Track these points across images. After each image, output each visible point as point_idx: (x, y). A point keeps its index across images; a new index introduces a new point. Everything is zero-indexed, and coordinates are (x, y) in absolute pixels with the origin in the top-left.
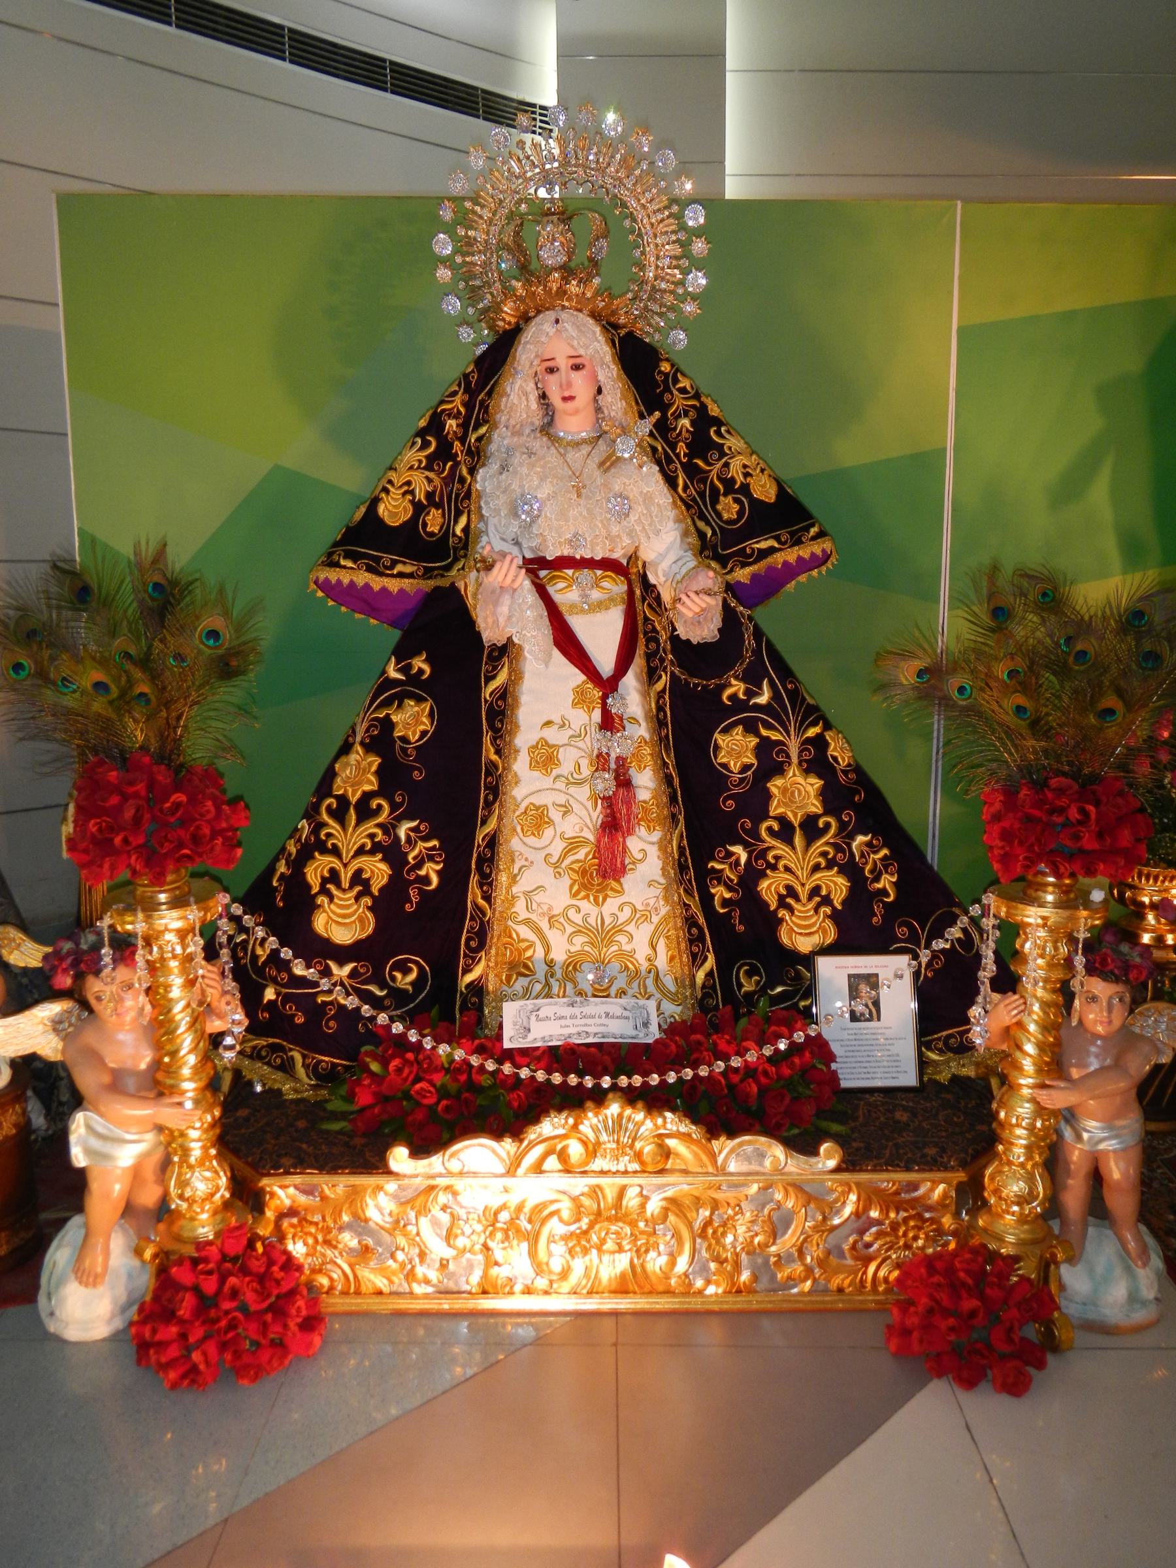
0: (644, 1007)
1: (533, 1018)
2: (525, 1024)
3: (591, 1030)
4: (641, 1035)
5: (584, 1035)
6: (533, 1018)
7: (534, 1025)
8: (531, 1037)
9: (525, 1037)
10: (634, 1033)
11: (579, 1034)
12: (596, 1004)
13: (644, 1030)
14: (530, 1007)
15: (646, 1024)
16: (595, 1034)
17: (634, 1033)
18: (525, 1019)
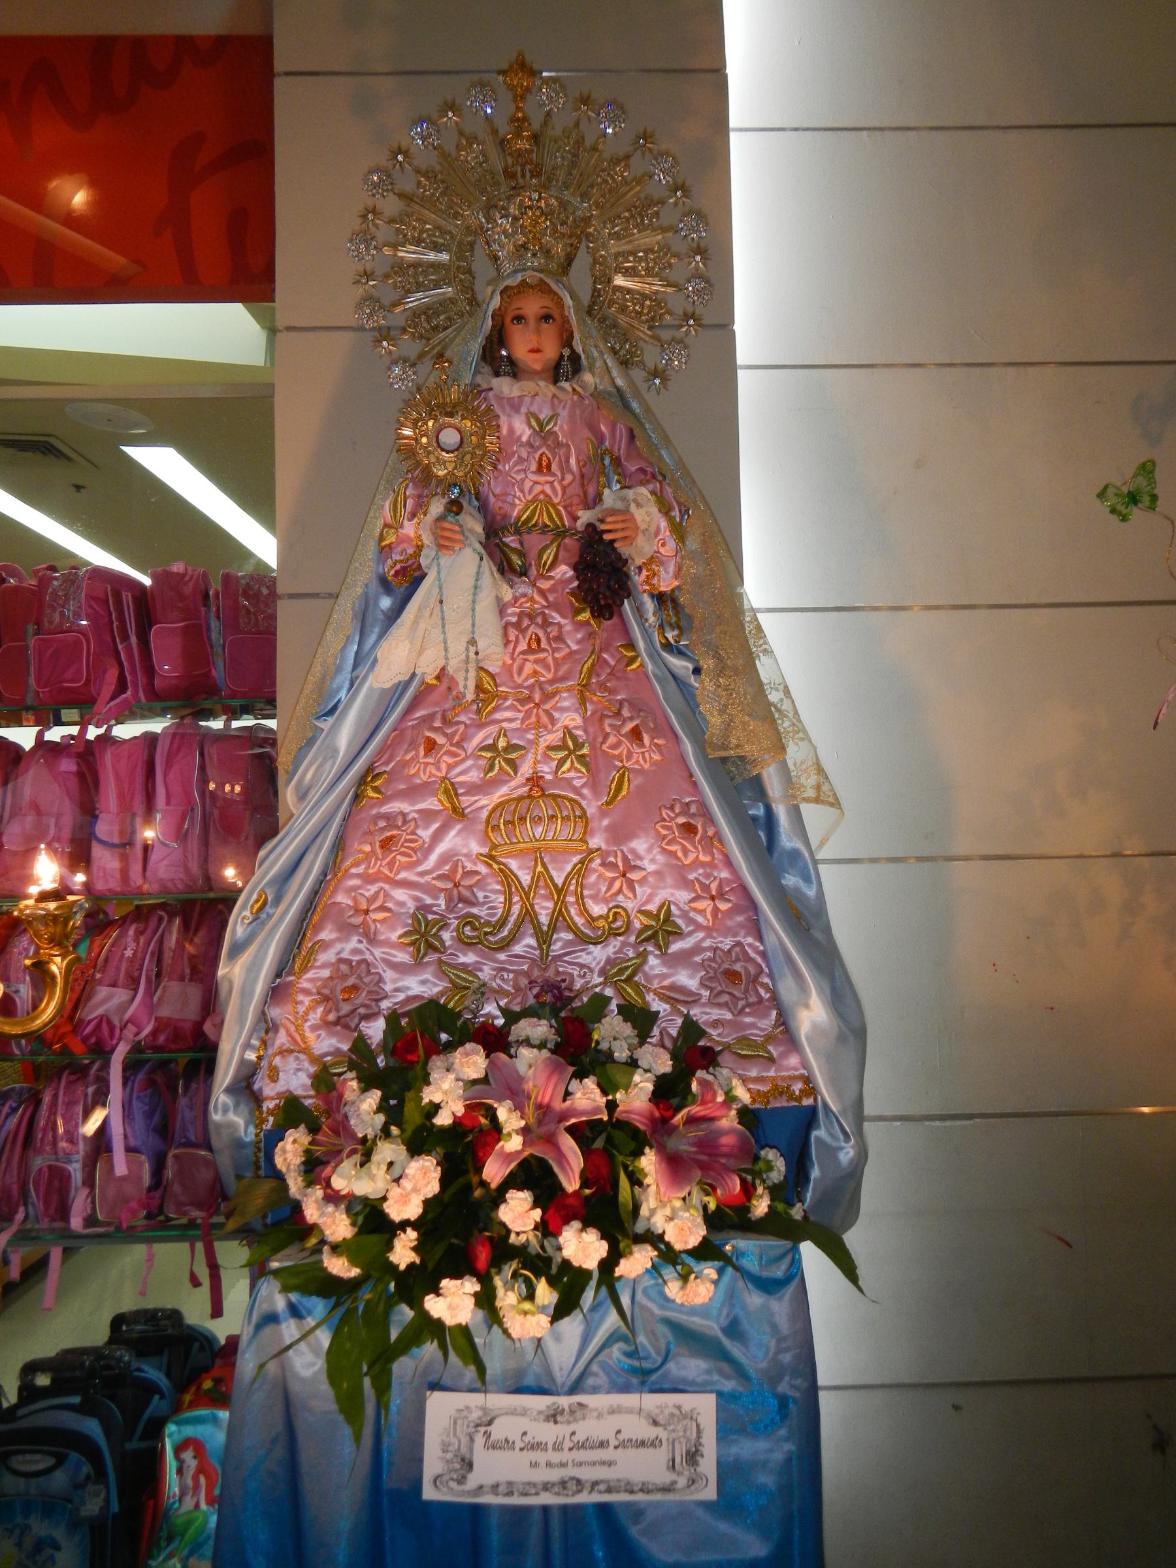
0: (691, 1416)
1: (480, 1440)
2: (464, 1450)
3: (587, 1474)
4: (682, 1482)
5: (572, 1486)
6: (480, 1440)
7: (480, 1455)
8: (473, 1481)
9: (462, 1480)
11: (563, 1483)
12: (600, 1416)
14: (476, 1415)
15: (693, 1457)
16: (595, 1484)
17: (666, 1477)
18: (465, 1440)
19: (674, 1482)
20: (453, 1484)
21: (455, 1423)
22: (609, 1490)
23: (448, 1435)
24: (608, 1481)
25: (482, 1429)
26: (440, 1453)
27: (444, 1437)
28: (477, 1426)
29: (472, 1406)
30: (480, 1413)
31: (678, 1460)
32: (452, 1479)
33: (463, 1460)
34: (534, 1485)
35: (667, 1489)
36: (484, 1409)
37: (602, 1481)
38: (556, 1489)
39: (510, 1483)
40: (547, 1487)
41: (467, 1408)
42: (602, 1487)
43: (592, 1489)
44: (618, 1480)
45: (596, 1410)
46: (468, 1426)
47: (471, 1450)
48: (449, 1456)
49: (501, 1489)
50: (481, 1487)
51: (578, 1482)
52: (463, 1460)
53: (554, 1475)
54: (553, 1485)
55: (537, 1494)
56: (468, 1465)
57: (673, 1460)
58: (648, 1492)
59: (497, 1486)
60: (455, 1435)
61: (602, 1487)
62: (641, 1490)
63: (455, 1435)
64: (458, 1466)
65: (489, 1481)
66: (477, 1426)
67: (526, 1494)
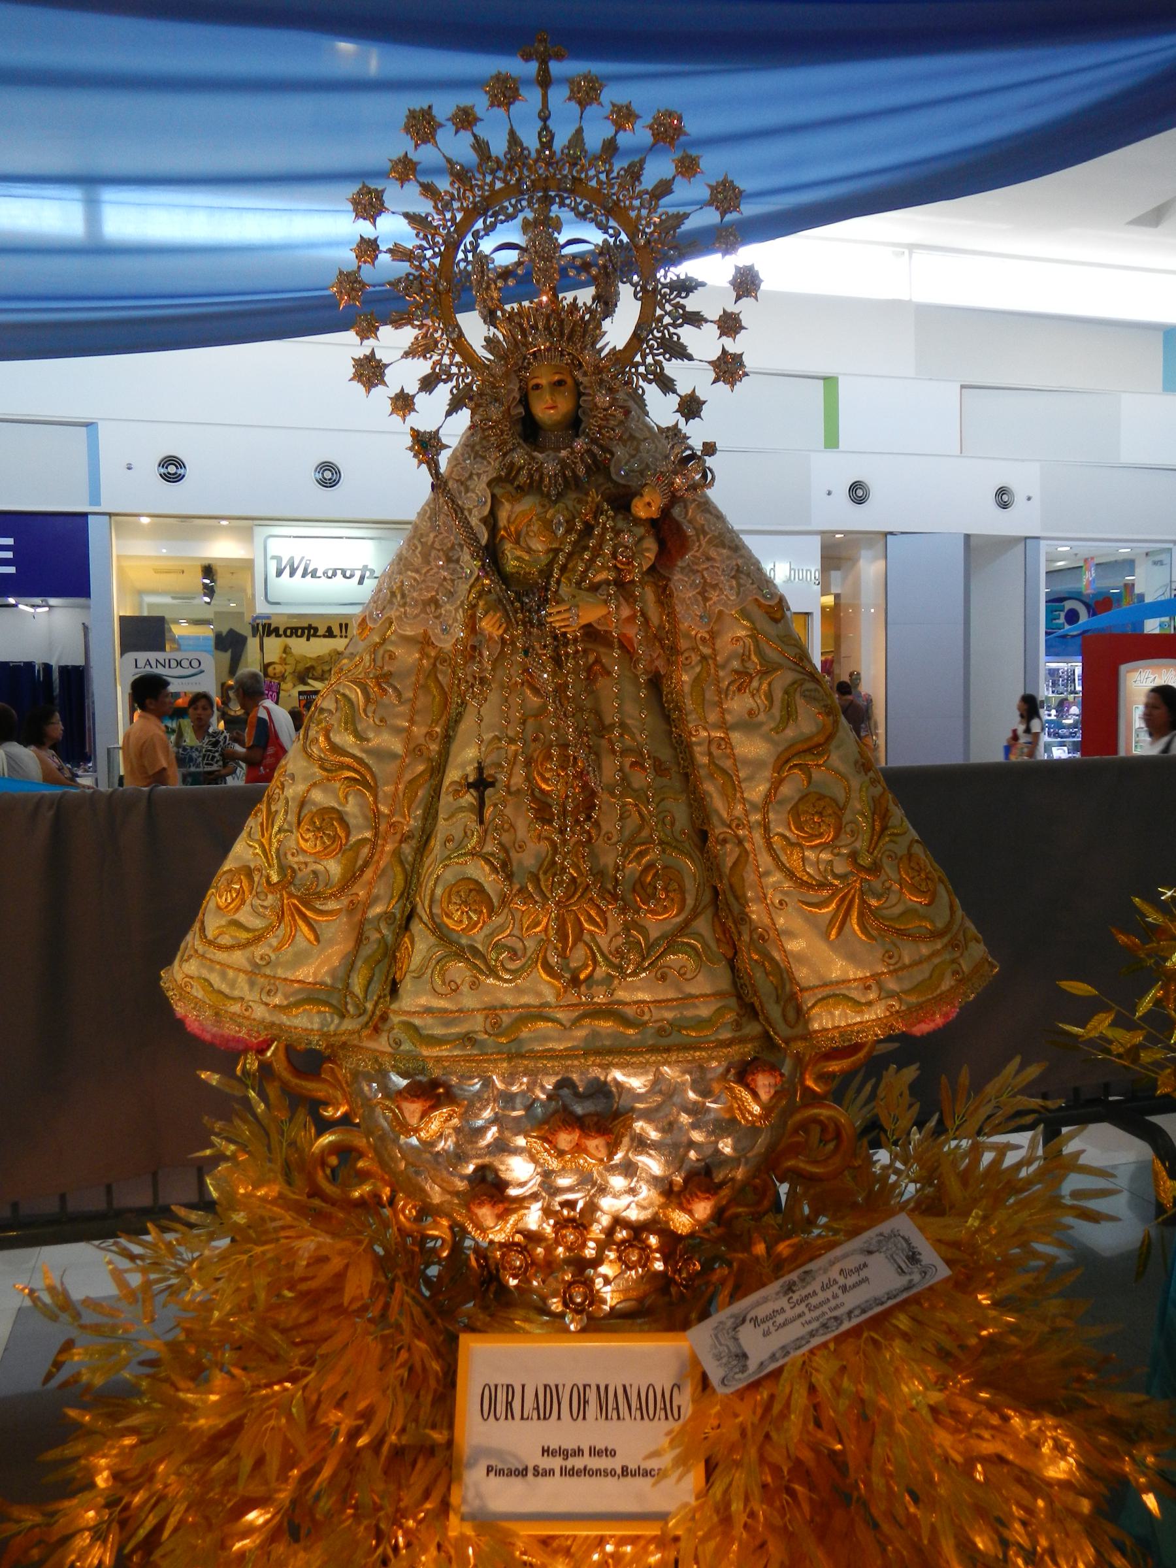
2: (734, 1349)
4: (916, 1277)
5: (833, 1324)
8: (752, 1365)
9: (744, 1369)
10: (903, 1281)
11: (824, 1326)
13: (916, 1269)
14: (729, 1323)
16: (850, 1314)
18: (731, 1343)
19: (911, 1281)
20: (740, 1376)
22: (864, 1311)
23: (716, 1347)
24: (859, 1306)
26: (717, 1363)
28: (735, 1329)
29: (724, 1319)
30: (732, 1320)
31: (903, 1266)
33: (737, 1356)
34: (802, 1338)
35: (907, 1289)
36: (732, 1316)
37: (854, 1309)
38: (821, 1332)
39: (783, 1348)
40: (812, 1334)
41: (721, 1323)
42: (857, 1312)
43: (850, 1318)
45: (820, 1269)
47: (740, 1346)
48: (724, 1360)
50: (762, 1364)
51: (836, 1318)
52: (737, 1356)
53: (815, 1325)
54: (817, 1330)
55: (808, 1342)
56: (745, 1356)
57: (900, 1267)
58: (895, 1297)
60: (721, 1344)
61: (857, 1312)
62: (889, 1298)
64: (735, 1362)
65: (765, 1356)
66: (735, 1329)
67: (800, 1347)
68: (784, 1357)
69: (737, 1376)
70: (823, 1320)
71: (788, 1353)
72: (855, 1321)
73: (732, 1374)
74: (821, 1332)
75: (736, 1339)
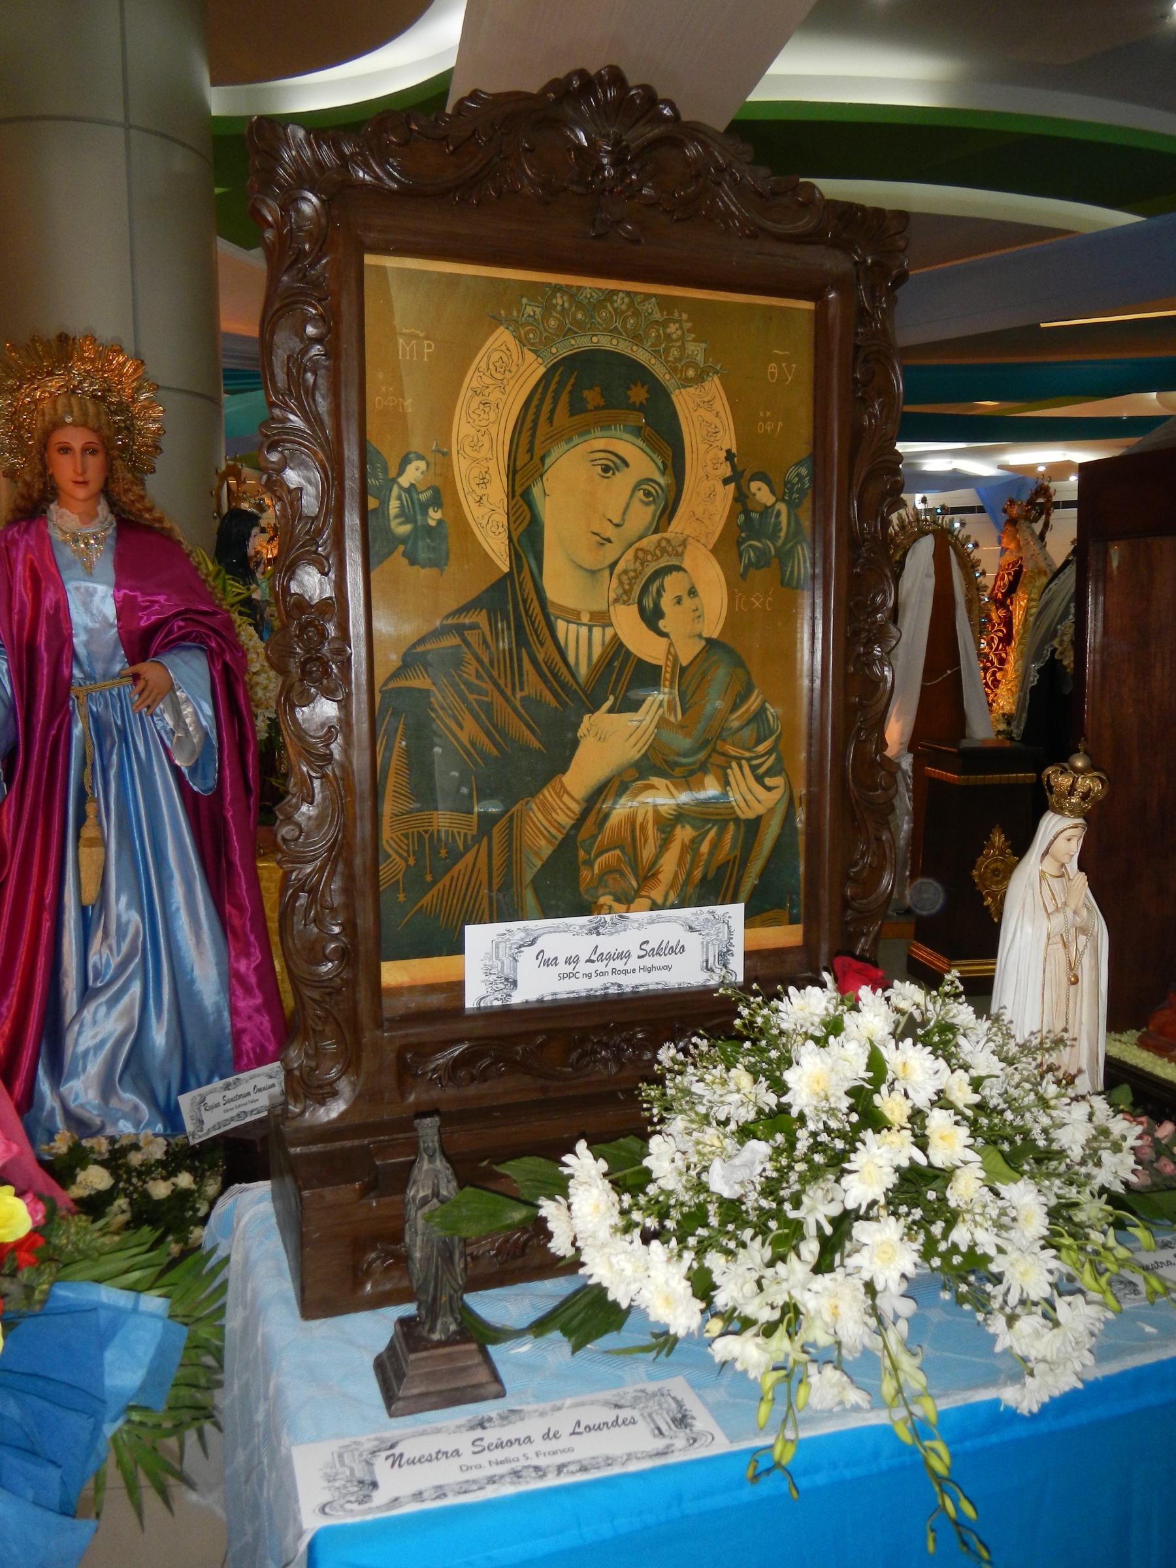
21: (340, 1456)
22: (584, 1469)
24: (579, 1461)
25: (384, 1454)
26: (326, 1484)
27: (328, 1471)
32: (349, 1502)
34: (474, 1482)
40: (492, 1480)
44: (594, 1458)
46: (361, 1455)
47: (372, 1473)
48: (337, 1484)
49: (425, 1495)
50: (396, 1499)
59: (420, 1493)
61: (573, 1468)
63: (343, 1464)
64: (356, 1489)
68: (438, 1497)
69: (349, 1506)
70: (517, 1466)
71: (445, 1495)
72: (566, 1480)
73: (342, 1502)
74: (508, 1479)
75: (369, 1464)
